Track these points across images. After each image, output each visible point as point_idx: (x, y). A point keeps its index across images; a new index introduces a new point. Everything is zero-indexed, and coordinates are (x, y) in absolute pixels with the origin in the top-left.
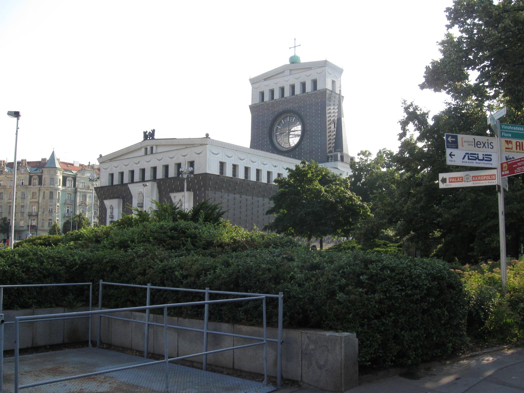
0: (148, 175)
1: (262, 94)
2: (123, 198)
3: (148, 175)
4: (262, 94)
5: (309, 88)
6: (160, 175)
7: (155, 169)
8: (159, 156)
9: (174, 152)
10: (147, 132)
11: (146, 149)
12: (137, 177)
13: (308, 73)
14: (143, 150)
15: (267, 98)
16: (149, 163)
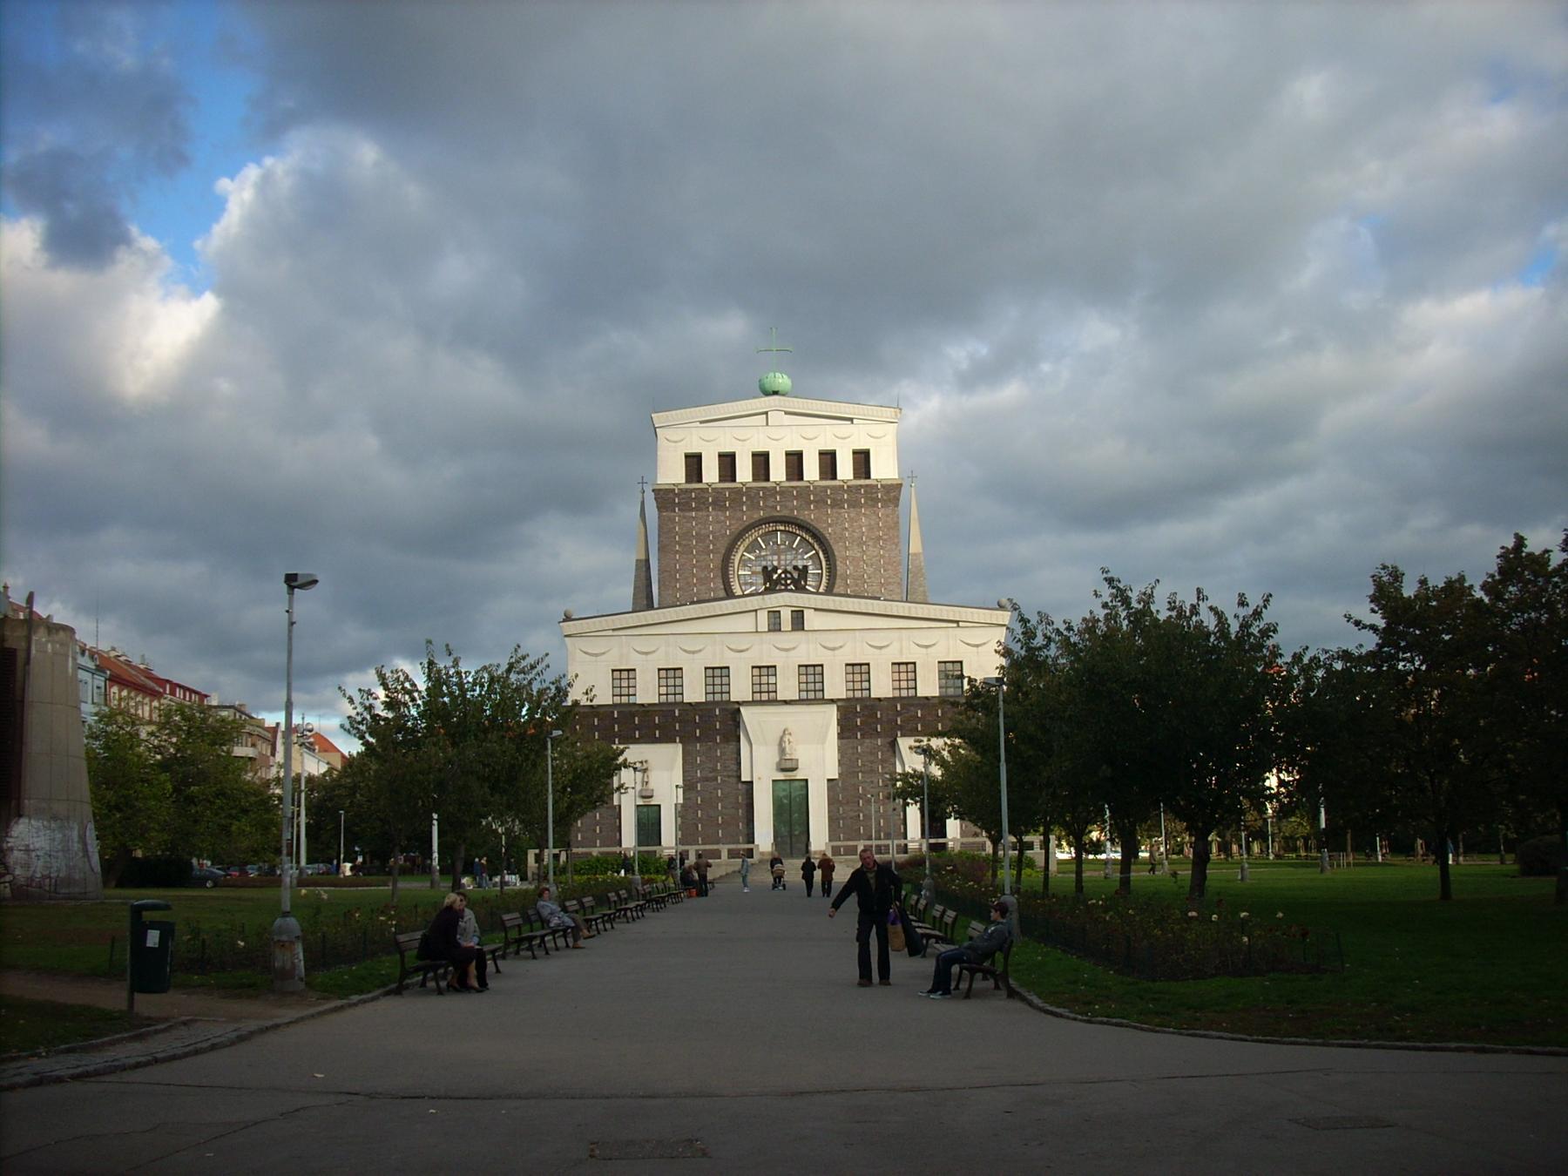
0: (788, 686)
1: (694, 463)
2: (687, 740)
3: (788, 686)
4: (694, 463)
5: (845, 470)
6: (836, 686)
7: (812, 673)
8: (833, 641)
9: (896, 634)
10: (775, 569)
11: (775, 615)
12: (740, 689)
13: (845, 428)
14: (763, 617)
15: (711, 473)
16: (792, 653)
